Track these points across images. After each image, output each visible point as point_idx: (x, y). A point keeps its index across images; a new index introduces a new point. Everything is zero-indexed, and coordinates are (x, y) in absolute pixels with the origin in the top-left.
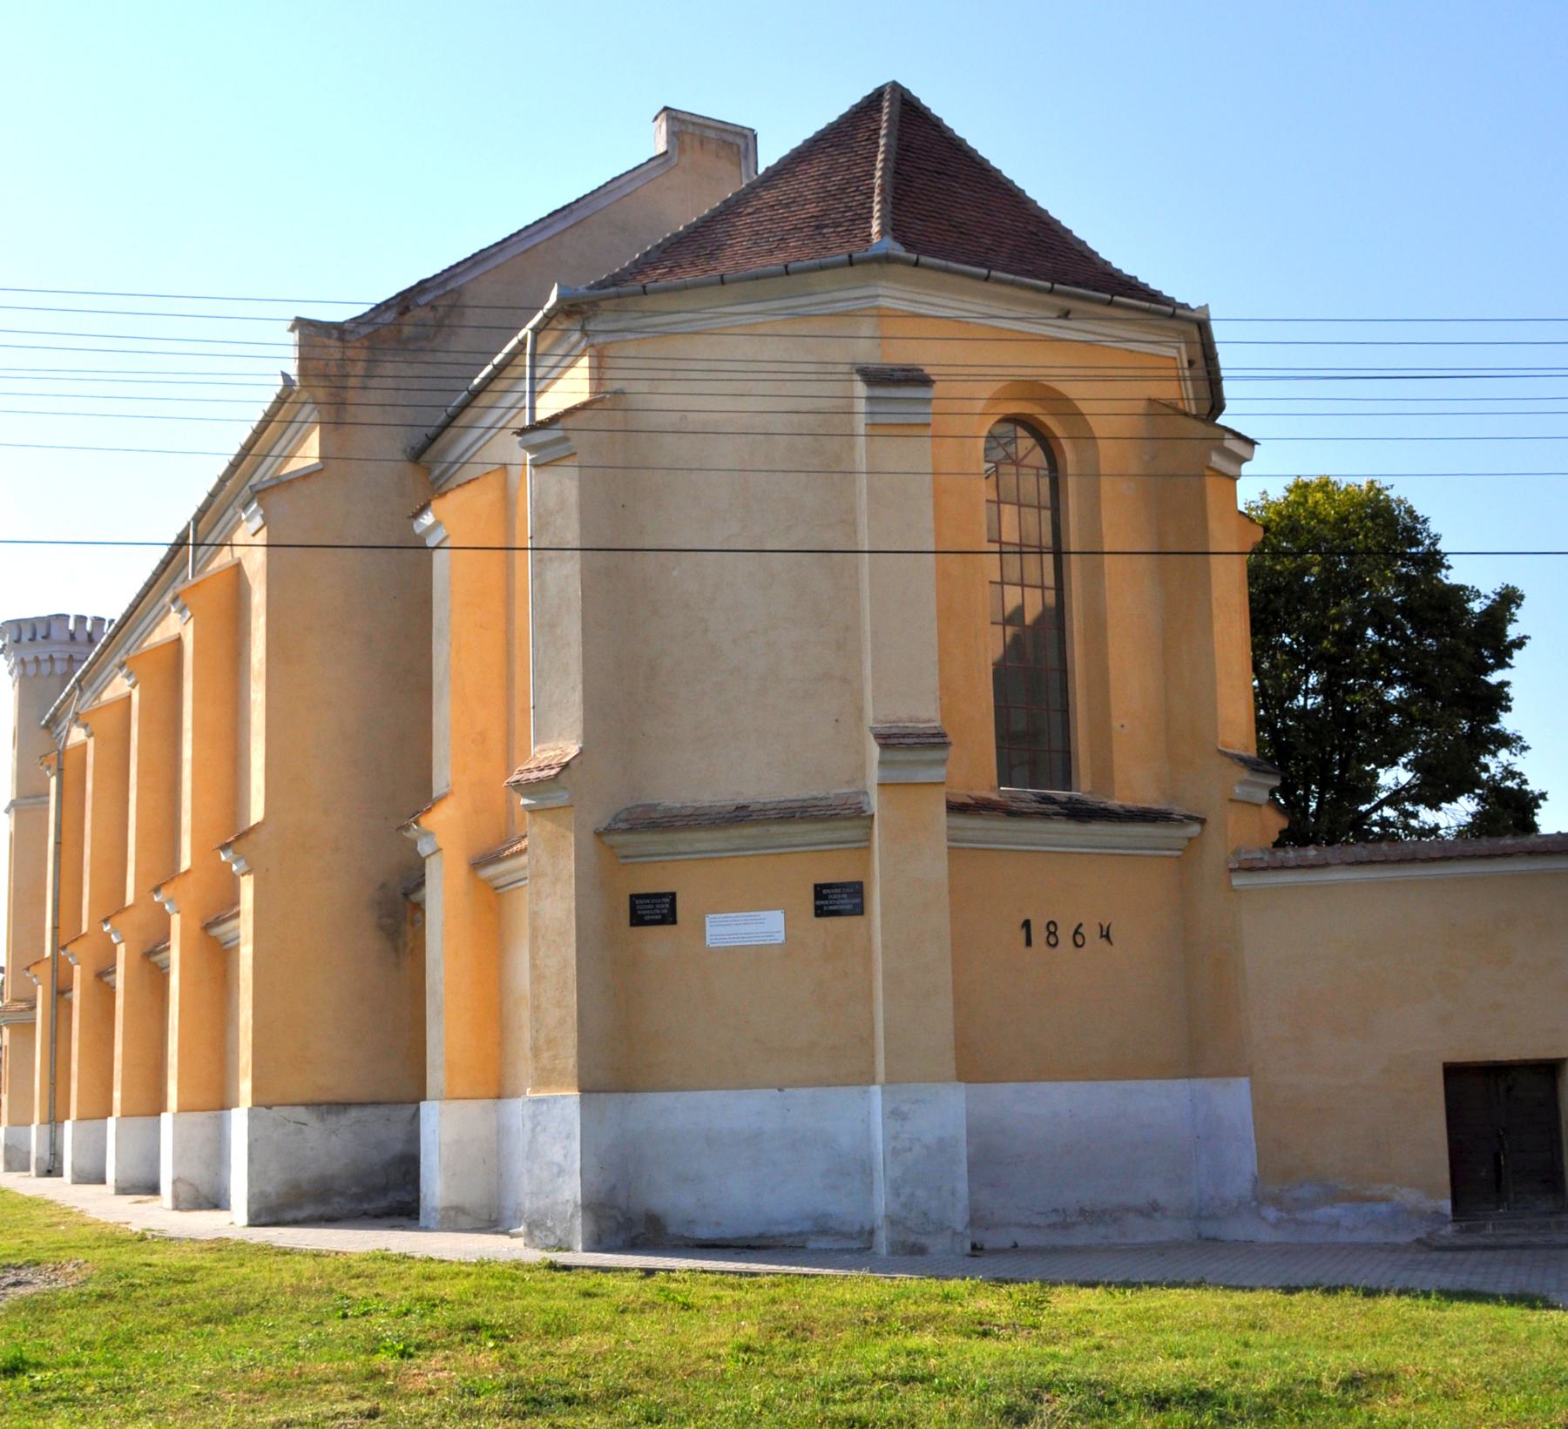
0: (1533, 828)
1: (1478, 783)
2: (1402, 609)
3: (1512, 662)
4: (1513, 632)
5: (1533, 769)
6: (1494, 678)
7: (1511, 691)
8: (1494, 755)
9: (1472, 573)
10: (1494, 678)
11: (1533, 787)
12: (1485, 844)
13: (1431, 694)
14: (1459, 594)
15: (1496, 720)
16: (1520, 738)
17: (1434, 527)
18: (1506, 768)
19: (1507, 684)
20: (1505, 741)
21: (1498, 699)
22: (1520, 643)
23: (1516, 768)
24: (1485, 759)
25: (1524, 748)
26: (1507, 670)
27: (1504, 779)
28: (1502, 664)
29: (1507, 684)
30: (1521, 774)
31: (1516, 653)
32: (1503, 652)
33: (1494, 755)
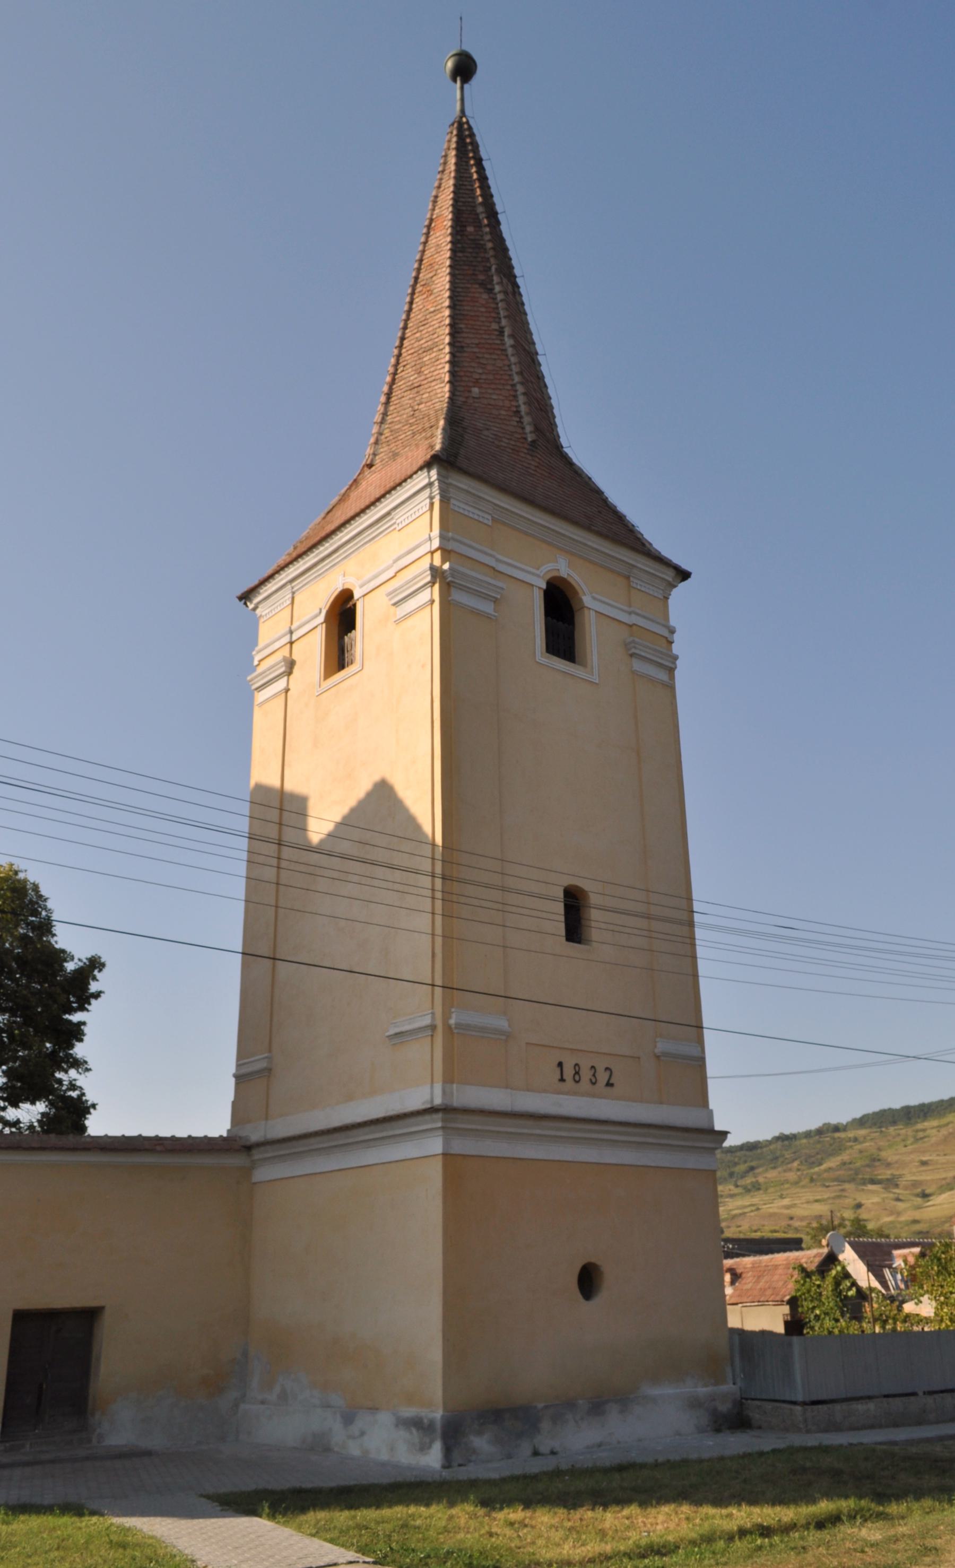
0: (84, 1129)
1: (52, 1091)
2: (18, 958)
3: (89, 1007)
4: (94, 987)
5: (89, 1085)
6: (76, 1017)
7: (86, 1029)
8: (66, 1072)
9: (73, 941)
10: (76, 1017)
11: (90, 1097)
12: (53, 1139)
13: (28, 1020)
14: (61, 956)
15: (72, 1046)
16: (86, 1062)
17: (49, 904)
18: (70, 1082)
19: (84, 1023)
20: (77, 1064)
21: (76, 1032)
22: (97, 995)
23: (78, 1083)
24: (58, 1075)
25: (88, 1070)
26: (85, 1013)
27: (69, 1089)
28: (82, 1008)
29: (84, 1023)
30: (81, 1088)
31: (93, 1001)
32: (84, 999)
33: (66, 1072)
